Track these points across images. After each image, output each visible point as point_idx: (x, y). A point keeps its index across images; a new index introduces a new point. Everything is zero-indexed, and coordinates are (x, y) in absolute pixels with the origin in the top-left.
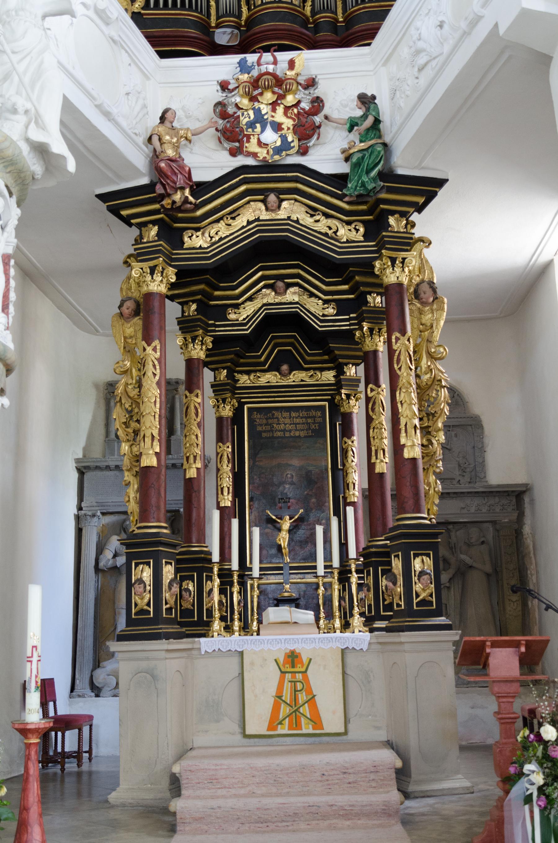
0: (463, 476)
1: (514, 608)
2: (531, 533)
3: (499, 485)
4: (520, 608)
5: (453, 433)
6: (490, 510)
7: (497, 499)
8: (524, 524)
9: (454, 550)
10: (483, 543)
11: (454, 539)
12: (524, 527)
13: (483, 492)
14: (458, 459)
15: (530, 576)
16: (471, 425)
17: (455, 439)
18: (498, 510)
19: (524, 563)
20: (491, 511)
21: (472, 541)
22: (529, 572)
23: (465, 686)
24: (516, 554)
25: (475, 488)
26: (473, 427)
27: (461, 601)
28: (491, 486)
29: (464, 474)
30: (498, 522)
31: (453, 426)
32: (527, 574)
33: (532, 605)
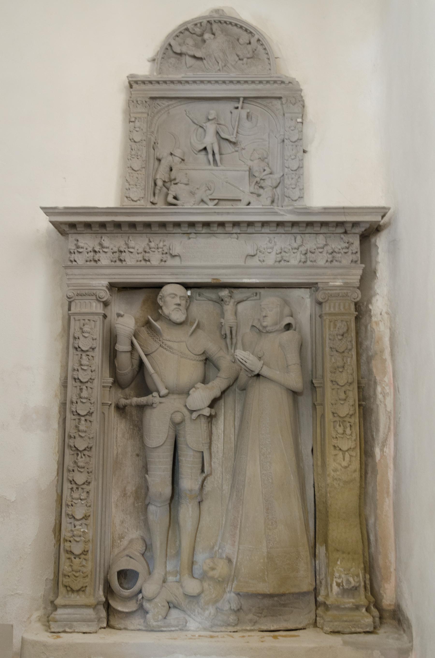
0: (259, 195)
1: (344, 464)
2: (387, 313)
3: (325, 208)
4: (356, 465)
5: (244, 113)
6: (305, 262)
7: (321, 240)
8: (376, 294)
9: (228, 340)
10: (288, 327)
11: (229, 318)
12: (374, 300)
13: (294, 224)
14: (250, 163)
15: (380, 396)
16: (280, 98)
17: (247, 124)
18: (322, 262)
19: (370, 371)
20: (309, 263)
21: (265, 324)
22: (379, 389)
23: (231, 629)
24: (354, 352)
25: (276, 213)
26: (284, 100)
27: (236, 446)
28: (308, 211)
29: (261, 191)
30: (320, 285)
31: (245, 98)
32: (375, 394)
33: (382, 456)
